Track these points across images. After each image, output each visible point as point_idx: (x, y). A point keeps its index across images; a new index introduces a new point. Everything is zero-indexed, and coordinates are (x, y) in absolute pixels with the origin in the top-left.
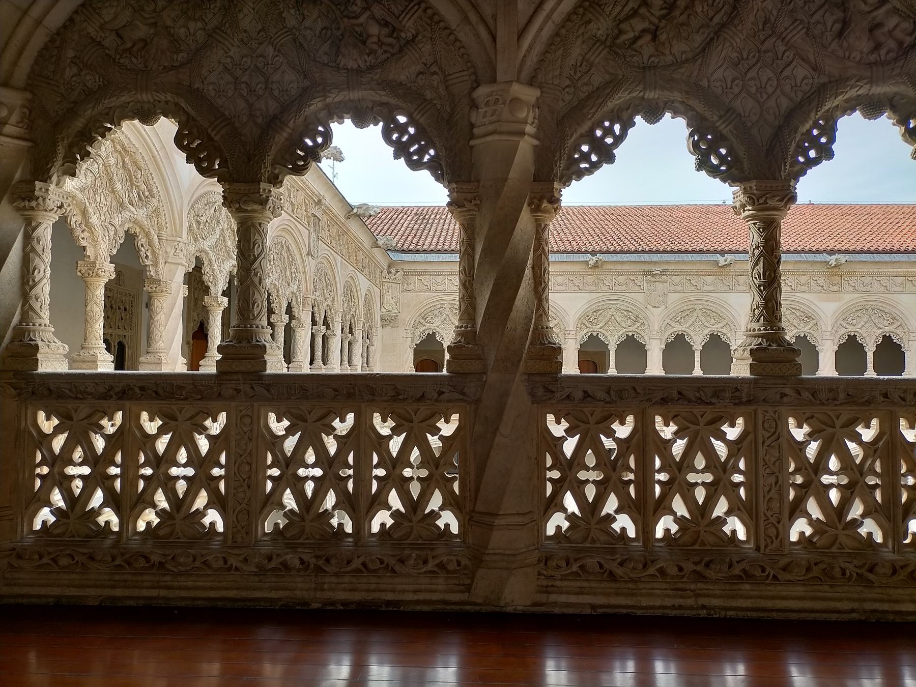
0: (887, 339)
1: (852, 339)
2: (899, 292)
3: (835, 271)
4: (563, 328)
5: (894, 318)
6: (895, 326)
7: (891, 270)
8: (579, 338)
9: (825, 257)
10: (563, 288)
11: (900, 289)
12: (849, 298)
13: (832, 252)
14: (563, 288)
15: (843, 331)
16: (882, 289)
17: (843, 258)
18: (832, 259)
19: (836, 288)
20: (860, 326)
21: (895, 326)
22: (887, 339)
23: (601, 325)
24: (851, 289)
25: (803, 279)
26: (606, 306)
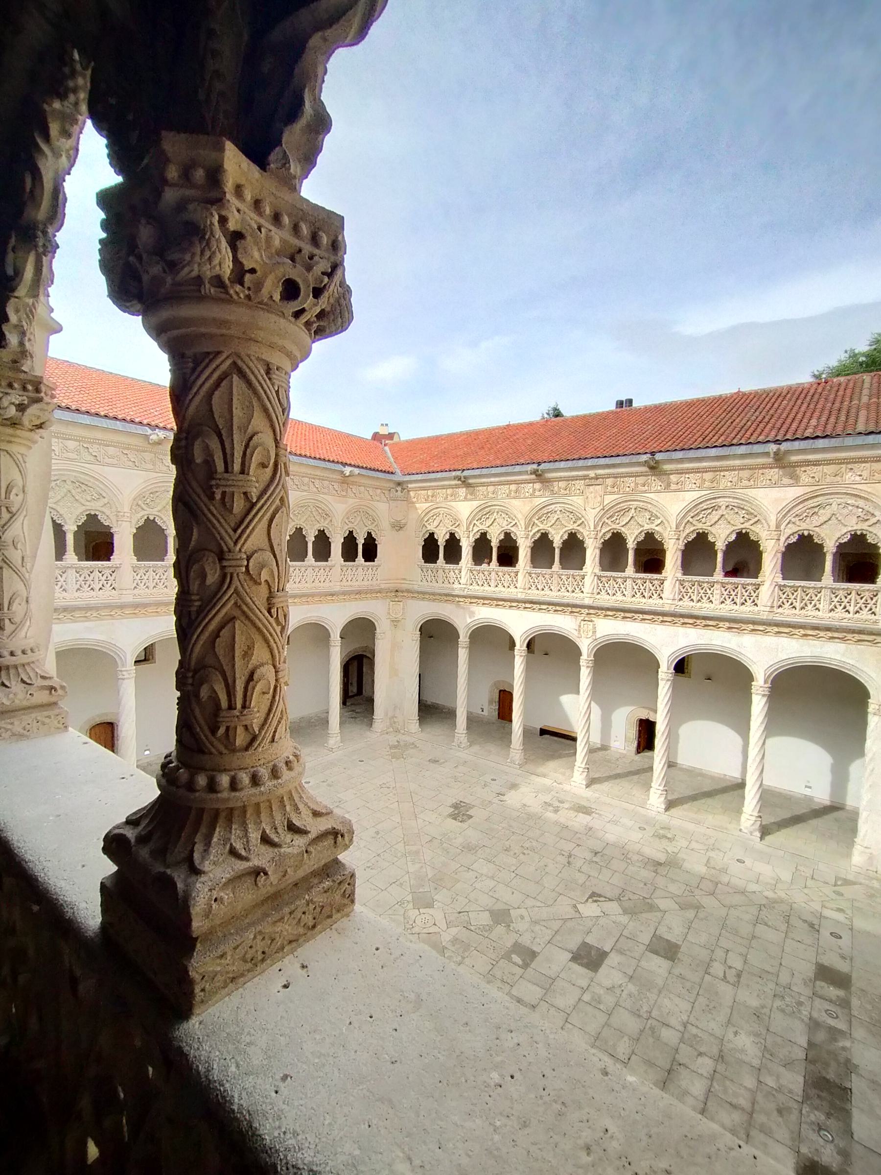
0: (369, 534)
1: (351, 533)
2: (378, 501)
3: (345, 480)
4: (114, 509)
5: (373, 520)
6: (374, 525)
7: (331, 476)
8: (134, 522)
9: (339, 467)
10: (115, 461)
11: (378, 498)
12: (352, 502)
13: (345, 464)
14: (115, 461)
15: (346, 527)
16: (369, 497)
17: (357, 471)
18: (347, 470)
19: (344, 493)
20: (355, 524)
21: (374, 525)
22: (369, 534)
23: (159, 508)
24: (353, 495)
25: (327, 482)
26: (163, 489)
